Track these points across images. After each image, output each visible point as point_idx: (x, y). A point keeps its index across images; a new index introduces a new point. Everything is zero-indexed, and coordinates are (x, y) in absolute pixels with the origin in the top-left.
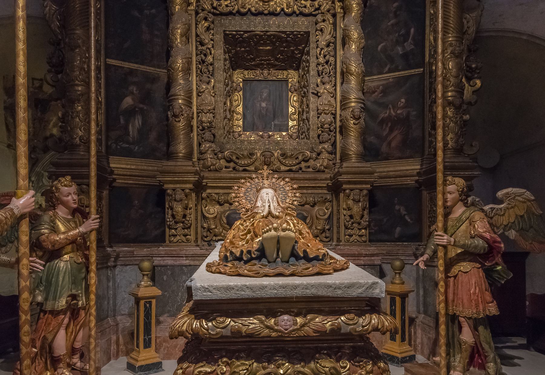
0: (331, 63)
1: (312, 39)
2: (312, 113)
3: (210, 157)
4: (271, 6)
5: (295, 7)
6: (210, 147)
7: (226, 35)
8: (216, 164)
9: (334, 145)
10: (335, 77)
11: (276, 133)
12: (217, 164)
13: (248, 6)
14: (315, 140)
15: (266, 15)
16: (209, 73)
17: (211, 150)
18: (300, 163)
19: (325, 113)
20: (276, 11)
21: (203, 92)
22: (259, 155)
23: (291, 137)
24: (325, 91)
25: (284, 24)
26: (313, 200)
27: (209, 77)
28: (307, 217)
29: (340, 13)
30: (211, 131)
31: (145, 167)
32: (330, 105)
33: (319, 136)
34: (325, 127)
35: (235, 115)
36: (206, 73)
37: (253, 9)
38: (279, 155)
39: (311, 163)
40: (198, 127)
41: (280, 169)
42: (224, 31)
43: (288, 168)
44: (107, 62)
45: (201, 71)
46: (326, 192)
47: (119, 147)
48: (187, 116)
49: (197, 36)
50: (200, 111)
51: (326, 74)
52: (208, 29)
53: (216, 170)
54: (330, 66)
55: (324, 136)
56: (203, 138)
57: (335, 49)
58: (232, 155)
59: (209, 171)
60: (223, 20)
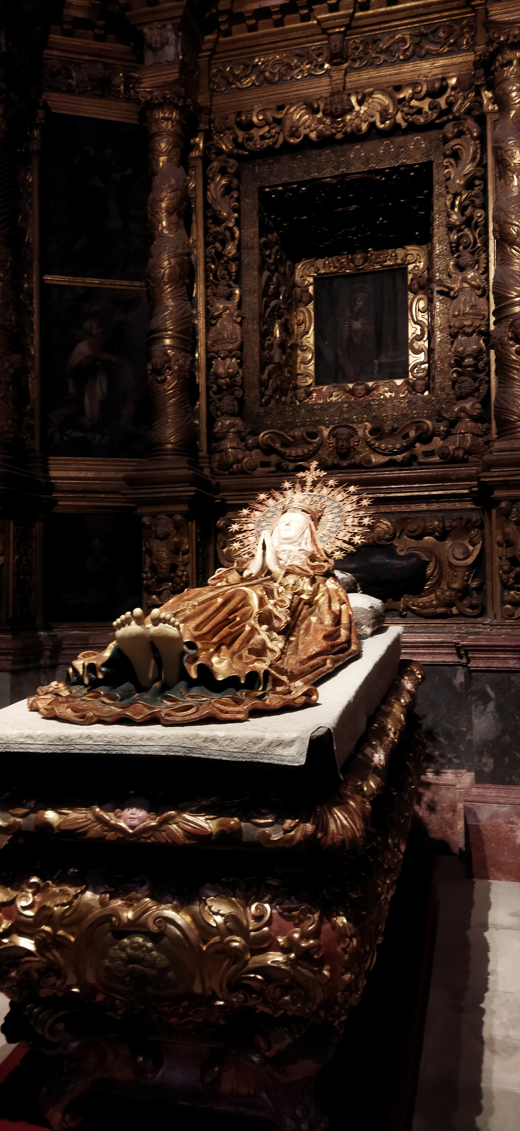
0: (477, 223)
1: (438, 176)
2: (439, 336)
3: (232, 445)
4: (349, 124)
5: (399, 116)
6: (232, 425)
7: (263, 197)
8: (243, 458)
9: (486, 401)
10: (487, 251)
11: (381, 383)
12: (246, 460)
13: (303, 131)
14: (448, 394)
15: (341, 142)
16: (231, 276)
17: (233, 432)
18: (411, 446)
19: (465, 334)
20: (360, 130)
21: (220, 316)
22: (326, 433)
23: (412, 387)
24: (465, 285)
25: (378, 154)
26: (441, 526)
27: (229, 286)
28: (427, 564)
29: (493, 112)
30: (233, 394)
31: (113, 473)
32: (476, 315)
33: (454, 382)
34: (464, 364)
35: (299, 352)
36: (224, 279)
37: (313, 135)
38: (367, 431)
39: (437, 442)
40: (208, 388)
41: (370, 461)
42: (261, 189)
43: (386, 459)
44: (46, 282)
45: (215, 276)
46: (469, 506)
47: (66, 438)
48: (178, 370)
49: (207, 206)
50: (213, 354)
51: (465, 248)
52: (228, 190)
53: (242, 472)
54: (476, 230)
55: (464, 384)
56: (218, 409)
57: (485, 191)
58: (272, 439)
59: (231, 473)
60: (257, 168)
